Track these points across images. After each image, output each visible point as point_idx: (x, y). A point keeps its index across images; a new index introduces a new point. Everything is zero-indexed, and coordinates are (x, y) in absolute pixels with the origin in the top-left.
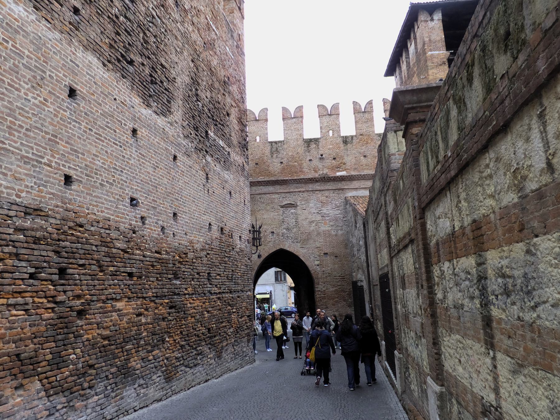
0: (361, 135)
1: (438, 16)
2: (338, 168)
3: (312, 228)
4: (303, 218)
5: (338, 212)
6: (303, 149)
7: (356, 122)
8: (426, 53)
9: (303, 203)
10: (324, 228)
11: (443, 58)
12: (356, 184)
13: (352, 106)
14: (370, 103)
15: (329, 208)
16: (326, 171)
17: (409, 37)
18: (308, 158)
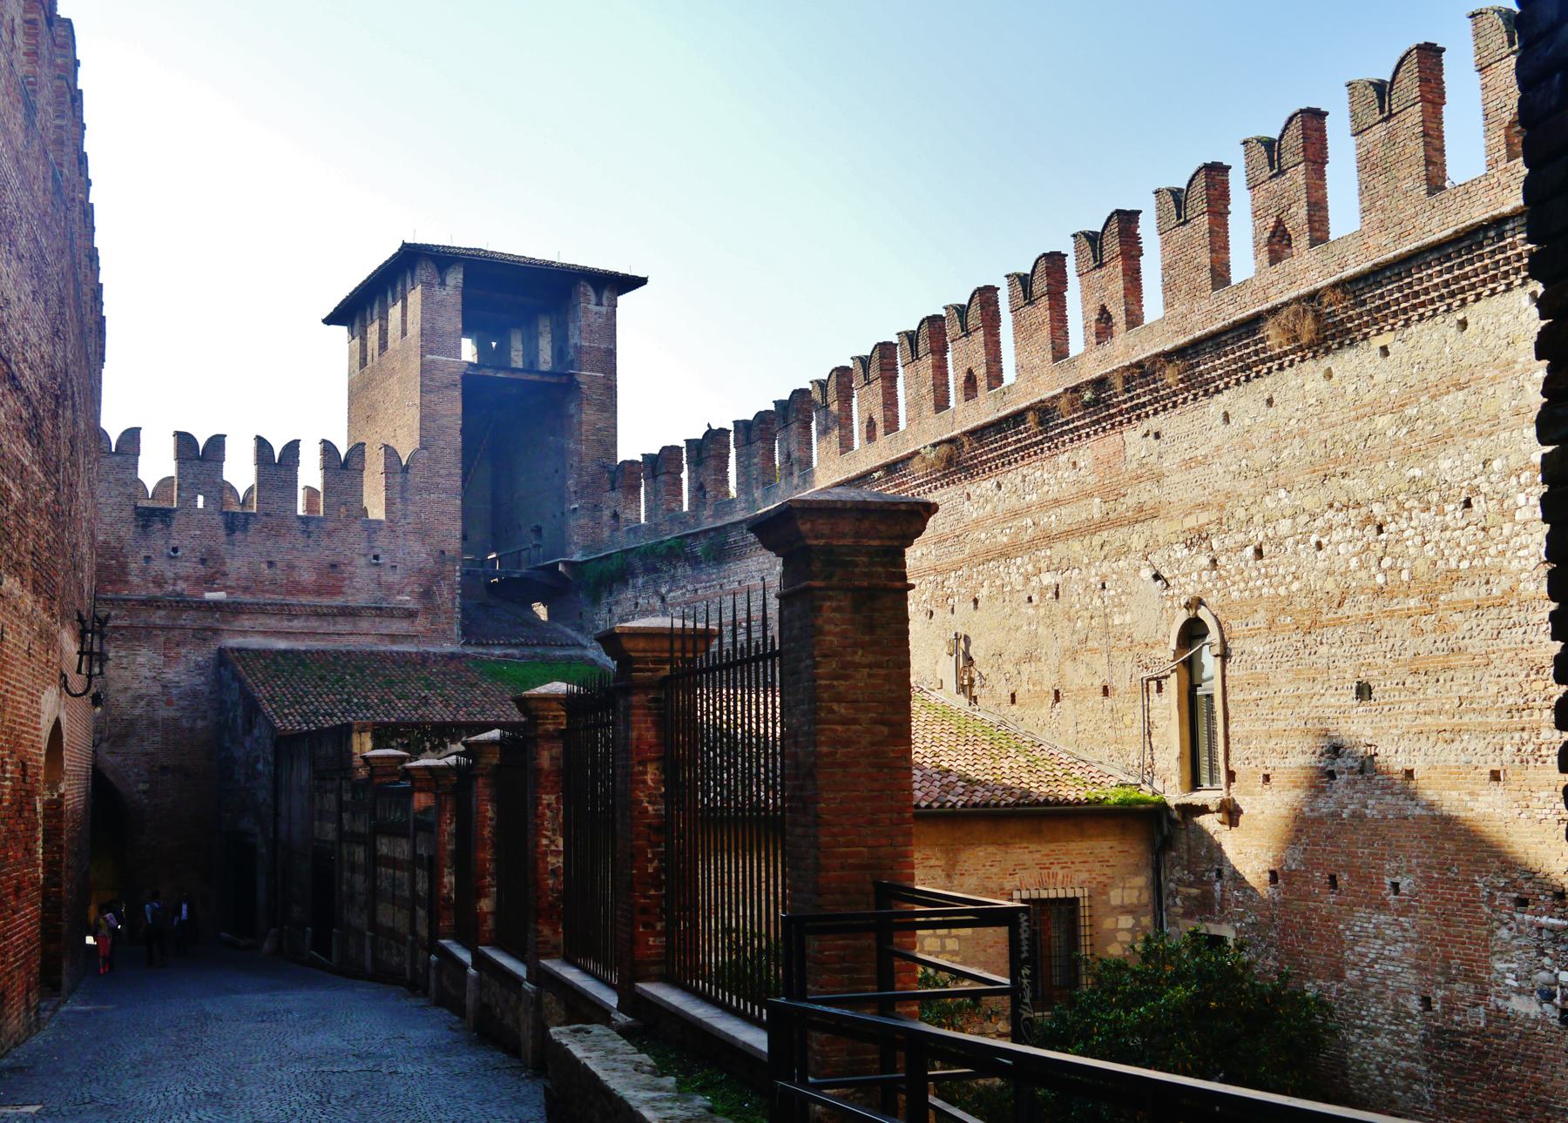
0: (268, 515)
1: (455, 278)
2: (209, 582)
3: (137, 712)
4: (120, 685)
5: (199, 680)
6: (132, 530)
9: (123, 653)
10: (163, 712)
12: (246, 622)
13: (252, 445)
14: (292, 448)
15: (181, 668)
16: (181, 586)
18: (143, 553)
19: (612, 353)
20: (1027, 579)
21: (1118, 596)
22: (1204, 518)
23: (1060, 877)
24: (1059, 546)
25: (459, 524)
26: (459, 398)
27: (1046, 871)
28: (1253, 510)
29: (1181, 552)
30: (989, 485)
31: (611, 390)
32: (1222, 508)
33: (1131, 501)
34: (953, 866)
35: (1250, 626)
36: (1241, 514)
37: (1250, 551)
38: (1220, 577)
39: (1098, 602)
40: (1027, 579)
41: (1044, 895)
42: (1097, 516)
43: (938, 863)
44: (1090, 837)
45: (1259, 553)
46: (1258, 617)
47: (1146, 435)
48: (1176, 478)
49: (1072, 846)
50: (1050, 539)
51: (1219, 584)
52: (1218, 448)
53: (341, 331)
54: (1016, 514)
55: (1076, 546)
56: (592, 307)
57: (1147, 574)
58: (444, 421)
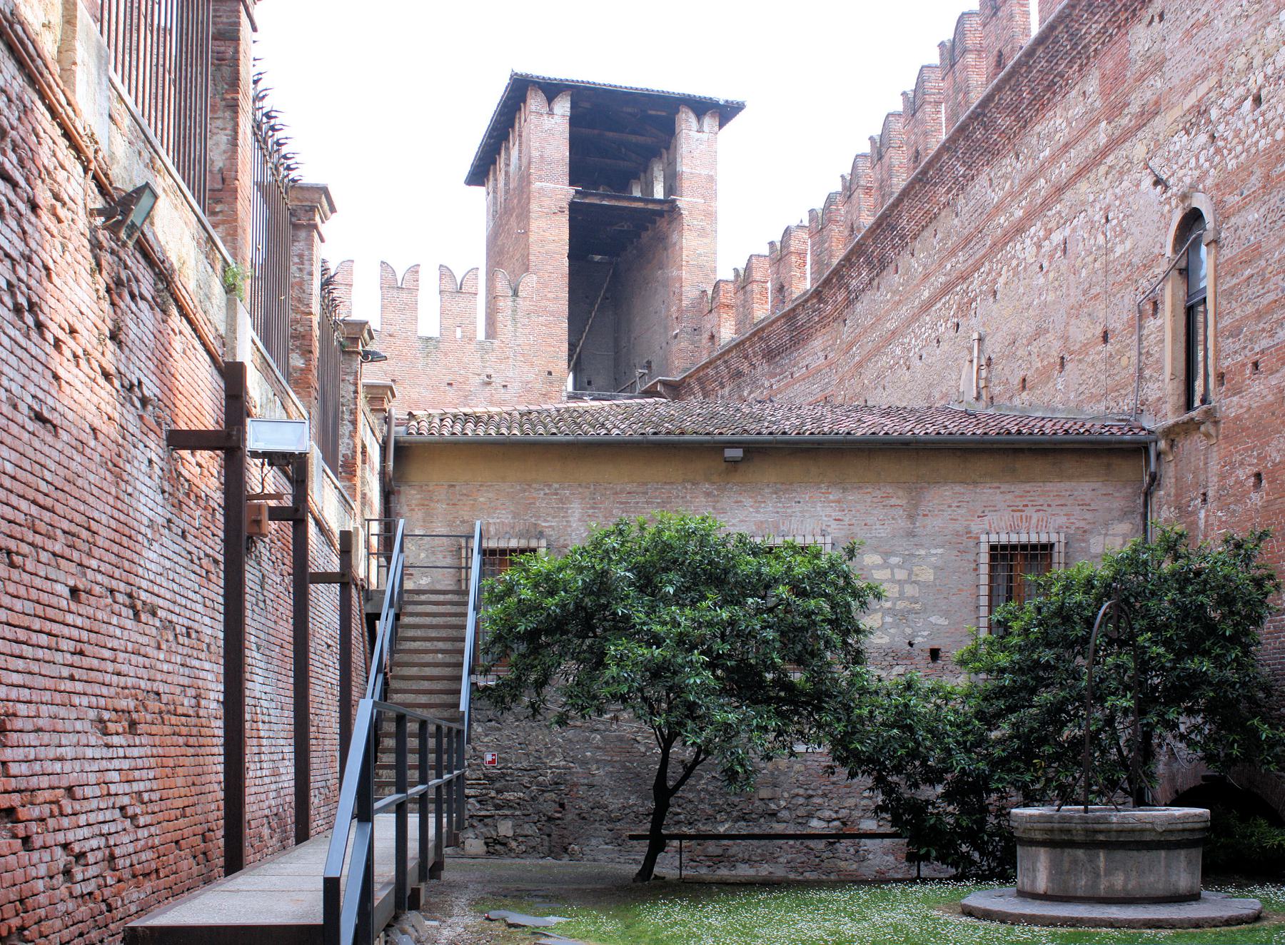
7: (383, 307)
8: (529, 183)
11: (561, 200)
17: (505, 138)
19: (711, 179)
20: (1039, 246)
21: (1120, 223)
22: (1202, 89)
23: (1034, 521)
25: (566, 345)
26: (567, 226)
27: (1019, 514)
28: (1254, 51)
29: (1181, 140)
31: (711, 215)
32: (1222, 66)
33: (1135, 108)
34: (916, 506)
35: (1246, 193)
36: (1241, 62)
37: (1248, 104)
38: (1218, 151)
39: (1101, 239)
40: (1039, 246)
41: (1014, 539)
43: (899, 502)
44: (1070, 478)
45: (1258, 100)
46: (1253, 178)
47: (1151, 23)
49: (1049, 486)
50: (1059, 190)
51: (1217, 159)
53: (479, 192)
54: (1030, 180)
55: (1083, 186)
56: (694, 134)
57: (1147, 182)
58: (552, 247)
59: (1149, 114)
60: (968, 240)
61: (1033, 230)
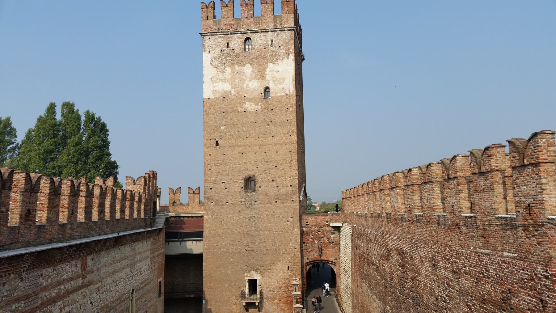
24: (71, 296)
30: (50, 270)
42: (80, 284)
48: (95, 273)
50: (69, 293)
52: (102, 266)
54: (59, 283)
55: (75, 296)
57: (89, 302)
59: (90, 283)
60: (27, 297)
61: (59, 303)
